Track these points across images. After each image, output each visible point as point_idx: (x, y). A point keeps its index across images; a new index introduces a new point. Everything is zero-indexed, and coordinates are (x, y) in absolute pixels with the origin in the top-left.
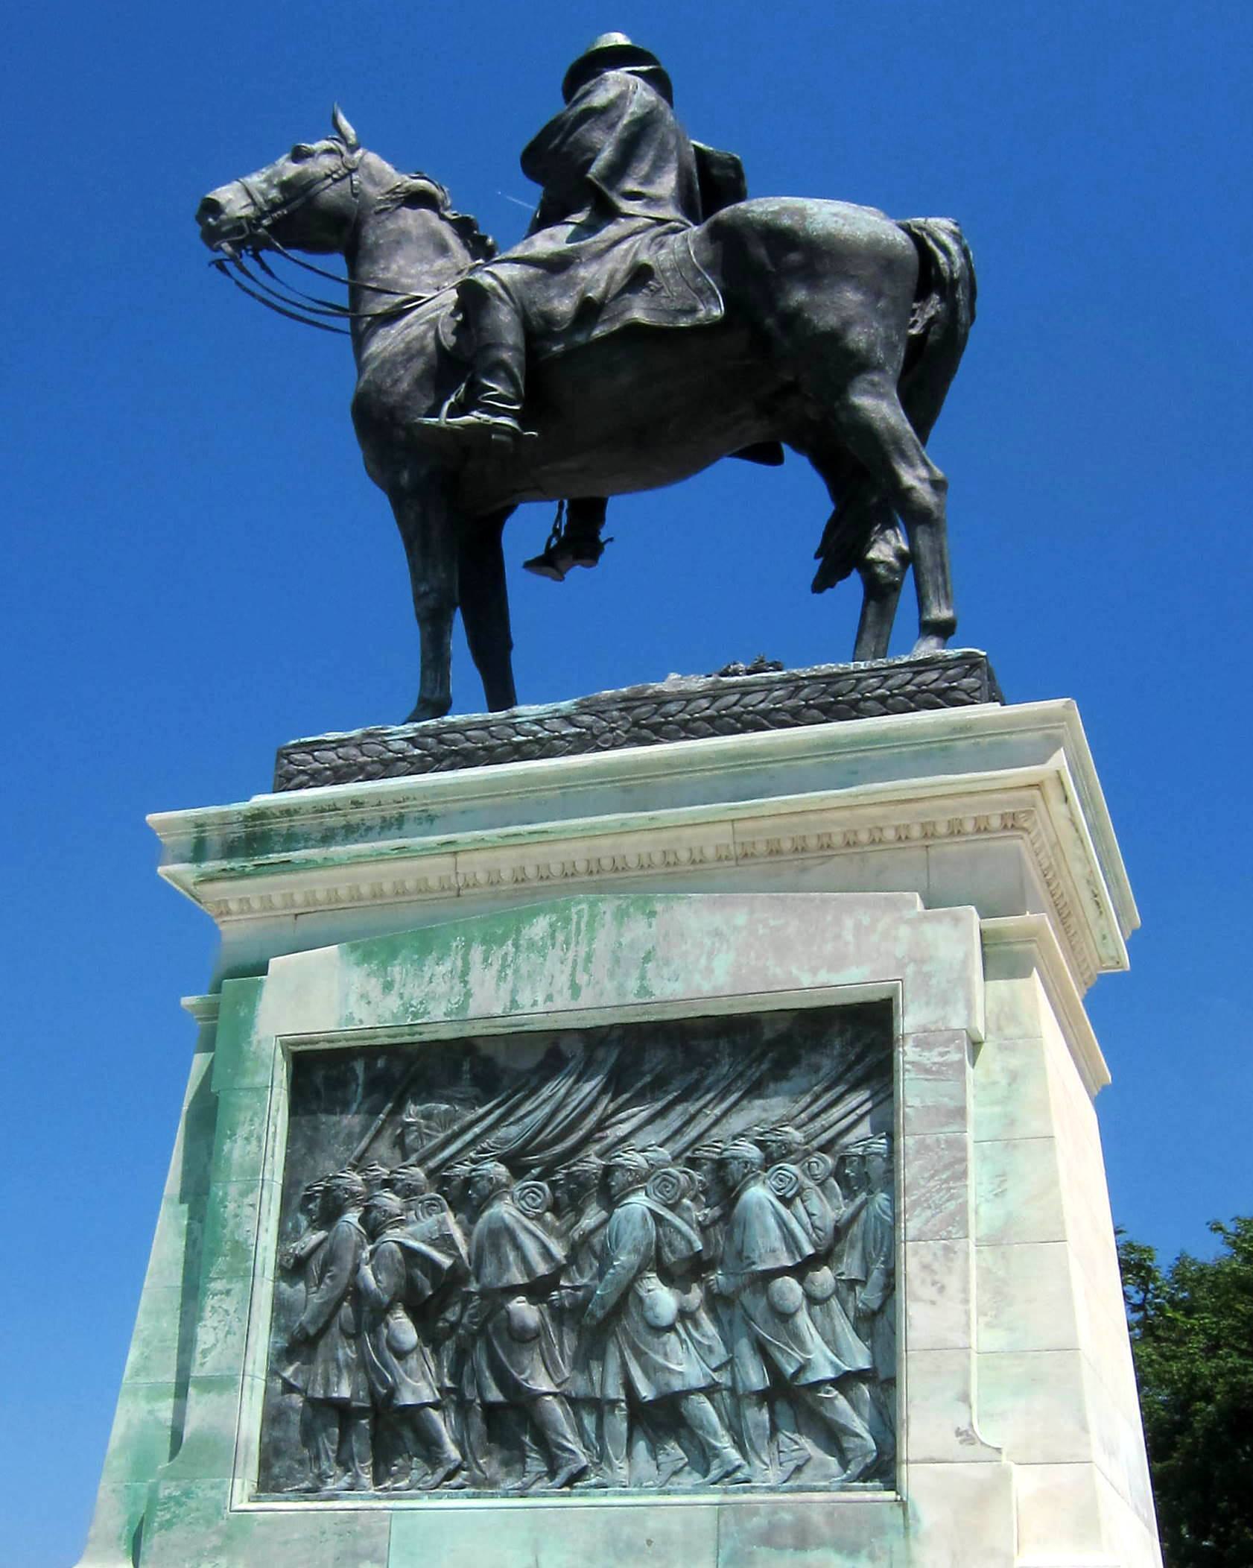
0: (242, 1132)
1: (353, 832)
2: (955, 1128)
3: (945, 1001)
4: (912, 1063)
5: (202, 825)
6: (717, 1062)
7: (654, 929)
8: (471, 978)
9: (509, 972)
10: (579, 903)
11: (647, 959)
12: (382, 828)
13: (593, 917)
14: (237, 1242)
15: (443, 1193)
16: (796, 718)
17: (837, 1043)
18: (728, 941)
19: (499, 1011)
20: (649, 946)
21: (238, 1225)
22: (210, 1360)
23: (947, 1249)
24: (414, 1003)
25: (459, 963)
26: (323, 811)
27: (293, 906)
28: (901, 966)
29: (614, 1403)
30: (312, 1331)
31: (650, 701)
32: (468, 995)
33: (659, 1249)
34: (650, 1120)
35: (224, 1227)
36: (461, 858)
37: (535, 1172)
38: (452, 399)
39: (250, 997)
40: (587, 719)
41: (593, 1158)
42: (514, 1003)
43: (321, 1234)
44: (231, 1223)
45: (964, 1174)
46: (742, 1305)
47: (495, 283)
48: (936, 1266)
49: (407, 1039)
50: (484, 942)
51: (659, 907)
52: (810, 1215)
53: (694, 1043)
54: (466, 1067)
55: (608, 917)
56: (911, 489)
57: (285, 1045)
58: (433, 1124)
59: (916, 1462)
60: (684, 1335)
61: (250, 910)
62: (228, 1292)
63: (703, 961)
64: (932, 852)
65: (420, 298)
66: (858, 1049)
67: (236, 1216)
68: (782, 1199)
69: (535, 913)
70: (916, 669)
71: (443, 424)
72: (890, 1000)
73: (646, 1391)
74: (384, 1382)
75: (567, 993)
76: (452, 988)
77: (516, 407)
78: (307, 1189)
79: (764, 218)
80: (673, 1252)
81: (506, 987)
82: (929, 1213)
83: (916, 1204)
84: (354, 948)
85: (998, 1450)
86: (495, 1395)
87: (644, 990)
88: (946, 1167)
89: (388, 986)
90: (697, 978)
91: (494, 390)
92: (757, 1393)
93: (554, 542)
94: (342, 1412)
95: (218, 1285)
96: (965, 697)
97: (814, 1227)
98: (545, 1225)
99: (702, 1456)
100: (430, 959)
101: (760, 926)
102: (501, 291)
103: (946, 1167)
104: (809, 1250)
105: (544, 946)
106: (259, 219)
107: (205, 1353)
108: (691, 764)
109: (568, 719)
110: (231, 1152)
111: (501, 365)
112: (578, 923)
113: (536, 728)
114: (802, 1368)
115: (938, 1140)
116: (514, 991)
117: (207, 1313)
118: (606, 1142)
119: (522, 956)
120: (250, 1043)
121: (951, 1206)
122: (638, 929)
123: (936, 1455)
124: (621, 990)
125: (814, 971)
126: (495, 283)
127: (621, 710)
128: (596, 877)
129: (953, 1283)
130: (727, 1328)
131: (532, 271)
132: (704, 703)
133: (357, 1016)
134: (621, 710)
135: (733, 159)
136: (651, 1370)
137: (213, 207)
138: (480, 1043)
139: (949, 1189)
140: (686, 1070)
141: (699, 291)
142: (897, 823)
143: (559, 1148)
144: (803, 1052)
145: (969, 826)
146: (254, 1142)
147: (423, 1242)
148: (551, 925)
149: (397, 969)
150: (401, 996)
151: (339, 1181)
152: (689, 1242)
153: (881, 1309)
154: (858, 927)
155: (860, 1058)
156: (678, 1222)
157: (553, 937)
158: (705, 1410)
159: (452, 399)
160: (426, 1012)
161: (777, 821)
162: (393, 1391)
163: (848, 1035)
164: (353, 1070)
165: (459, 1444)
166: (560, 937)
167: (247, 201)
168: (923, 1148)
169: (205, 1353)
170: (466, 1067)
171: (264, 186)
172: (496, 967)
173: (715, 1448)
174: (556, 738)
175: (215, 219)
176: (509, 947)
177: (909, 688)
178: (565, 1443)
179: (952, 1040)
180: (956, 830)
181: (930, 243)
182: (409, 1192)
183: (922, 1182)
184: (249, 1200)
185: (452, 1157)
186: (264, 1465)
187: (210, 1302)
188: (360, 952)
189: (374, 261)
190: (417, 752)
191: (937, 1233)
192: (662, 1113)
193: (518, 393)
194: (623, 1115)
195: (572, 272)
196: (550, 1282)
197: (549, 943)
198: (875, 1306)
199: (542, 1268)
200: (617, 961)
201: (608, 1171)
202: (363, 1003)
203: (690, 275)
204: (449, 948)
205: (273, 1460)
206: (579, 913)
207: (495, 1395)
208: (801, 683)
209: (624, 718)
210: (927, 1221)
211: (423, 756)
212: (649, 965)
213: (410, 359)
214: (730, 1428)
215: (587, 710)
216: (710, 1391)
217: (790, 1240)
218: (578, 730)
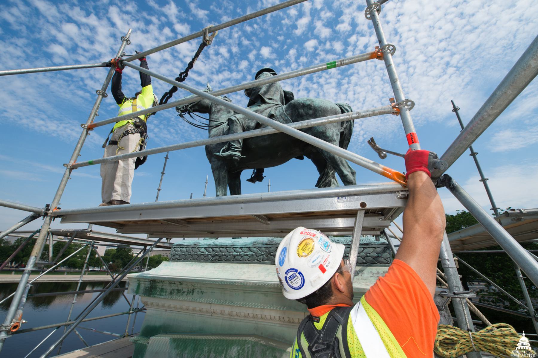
1: (179, 292)
12: (187, 293)
31: (274, 246)
38: (224, 148)
40: (255, 249)
47: (236, 119)
56: (347, 175)
71: (220, 155)
77: (240, 150)
79: (303, 102)
93: (253, 175)
102: (237, 121)
106: (188, 105)
113: (240, 250)
126: (236, 119)
127: (265, 247)
134: (265, 247)
135: (292, 93)
159: (224, 148)
181: (343, 108)
190: (207, 253)
193: (241, 146)
215: (254, 246)
218: (252, 253)
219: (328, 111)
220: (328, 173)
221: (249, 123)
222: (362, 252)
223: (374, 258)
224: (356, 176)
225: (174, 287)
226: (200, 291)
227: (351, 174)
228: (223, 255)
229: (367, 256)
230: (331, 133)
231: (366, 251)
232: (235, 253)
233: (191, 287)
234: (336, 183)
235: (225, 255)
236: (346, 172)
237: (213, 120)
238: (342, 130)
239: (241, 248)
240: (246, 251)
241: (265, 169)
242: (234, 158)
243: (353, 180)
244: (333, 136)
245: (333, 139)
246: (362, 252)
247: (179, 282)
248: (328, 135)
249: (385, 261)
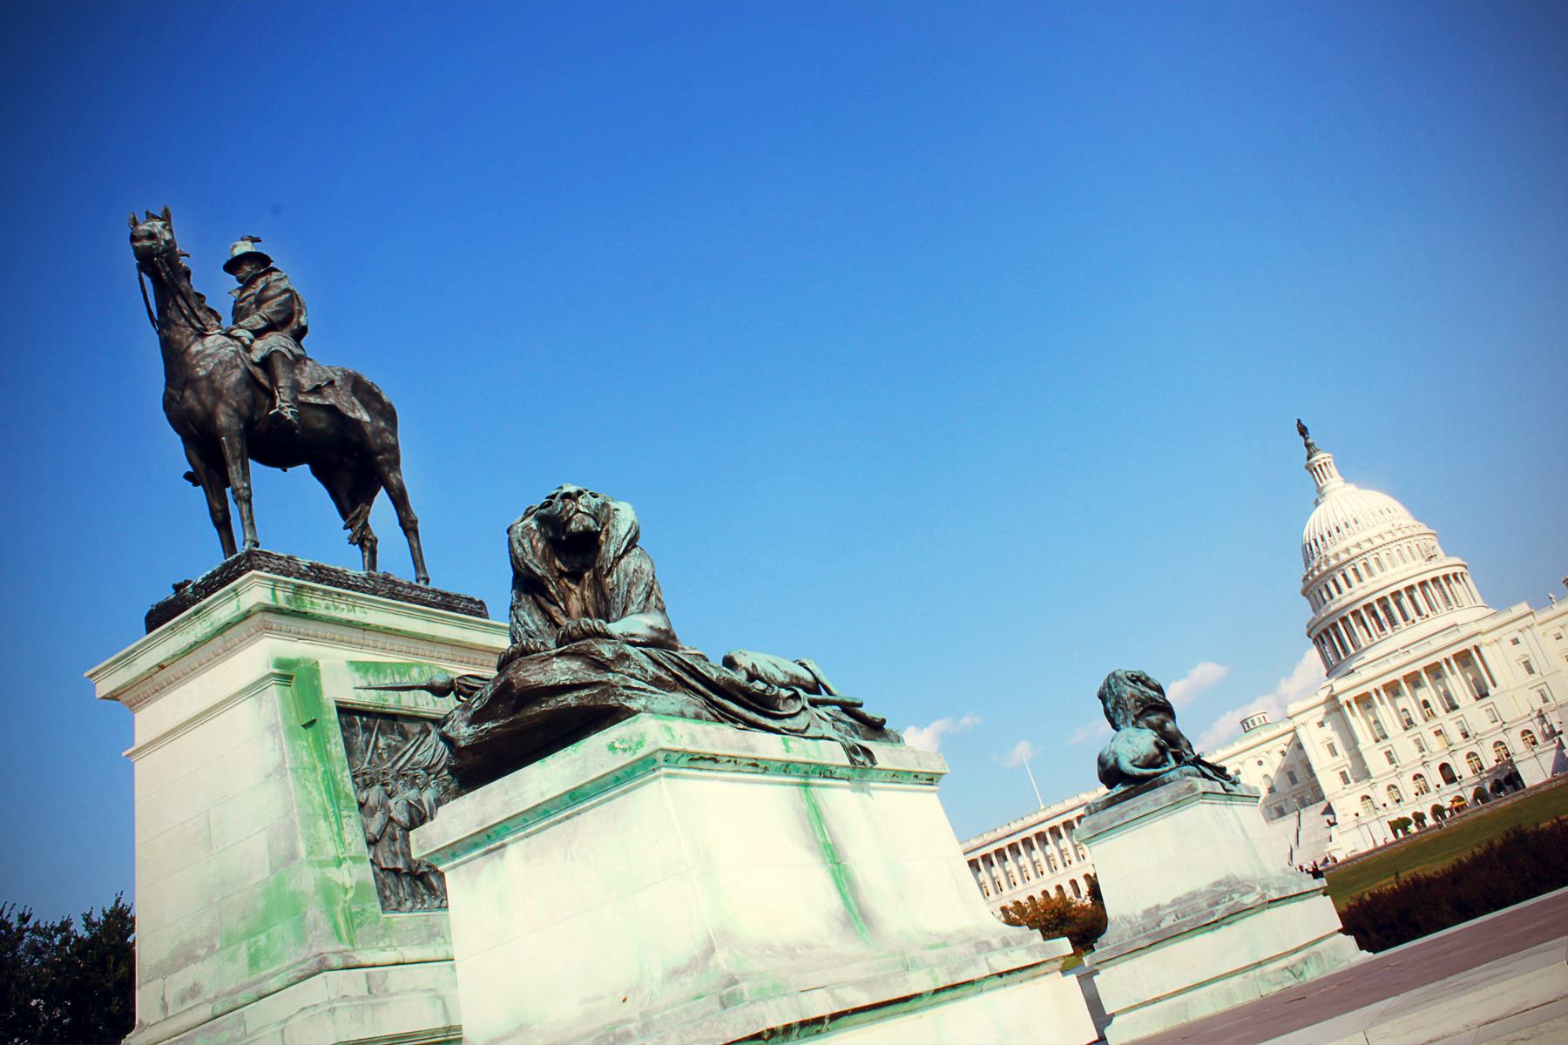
0: (333, 741)
42: (416, 703)
44: (341, 784)
107: (350, 844)
164: (355, 720)
169: (350, 844)
185: (402, 767)
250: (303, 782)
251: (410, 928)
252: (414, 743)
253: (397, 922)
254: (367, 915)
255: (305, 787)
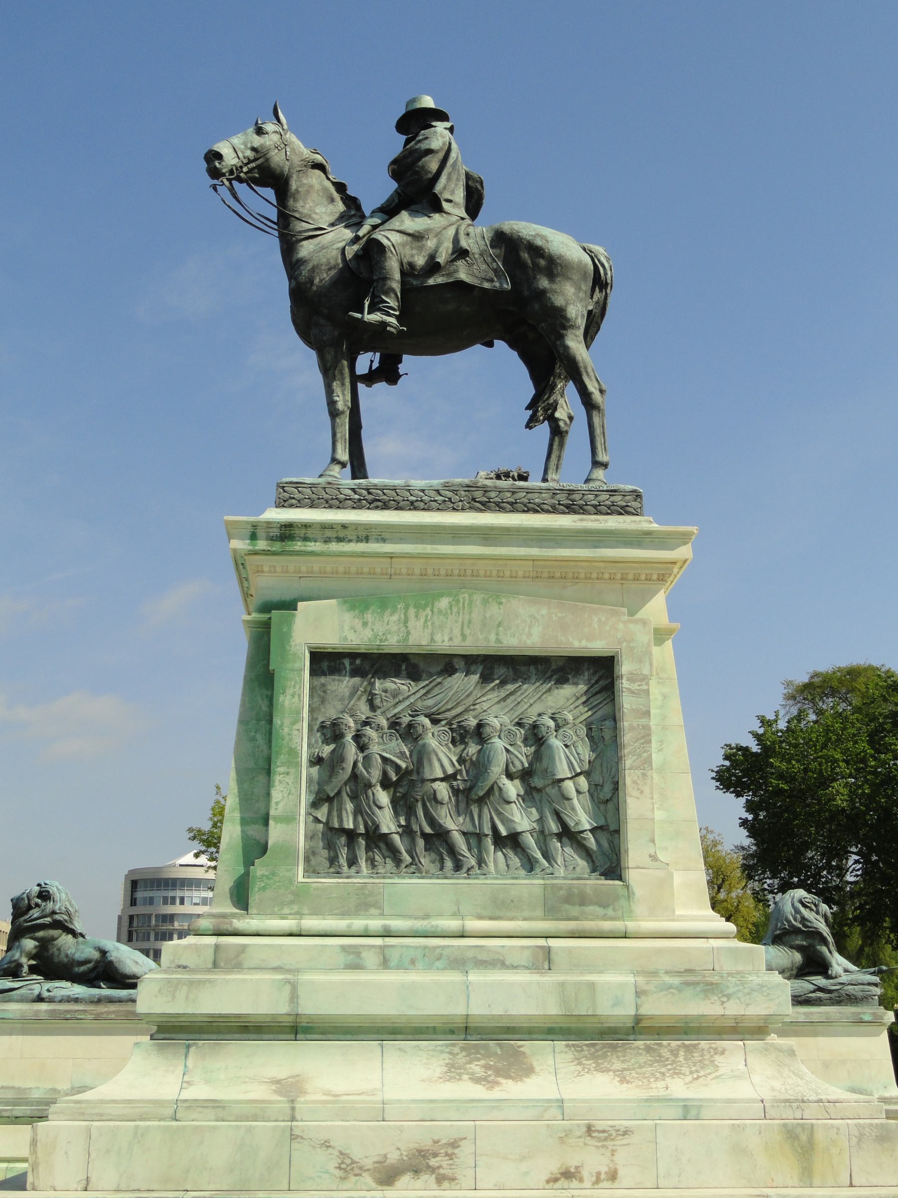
0: (289, 691)
2: (646, 720)
3: (640, 661)
4: (627, 688)
5: (255, 526)
6: (530, 677)
7: (502, 611)
8: (410, 624)
9: (429, 624)
10: (464, 593)
11: (499, 625)
13: (471, 602)
14: (291, 748)
15: (396, 730)
16: (554, 510)
17: (586, 674)
18: (538, 621)
19: (426, 644)
20: (500, 619)
21: (291, 740)
22: (280, 806)
23: (644, 775)
24: (380, 634)
25: (403, 616)
26: (325, 528)
27: (299, 572)
28: (620, 643)
29: (487, 835)
30: (332, 795)
32: (408, 633)
33: (507, 766)
34: (499, 702)
35: (283, 740)
36: (394, 560)
37: (443, 723)
39: (289, 623)
40: (447, 492)
41: (472, 719)
42: (432, 640)
43: (332, 746)
44: (287, 738)
45: (650, 742)
46: (546, 793)
47: (389, 244)
48: (639, 782)
49: (375, 651)
50: (415, 607)
51: (504, 600)
52: (578, 754)
53: (518, 667)
54: (404, 667)
55: (478, 603)
57: (309, 648)
58: (388, 695)
59: (632, 868)
60: (519, 806)
61: (275, 572)
62: (288, 773)
63: (527, 630)
64: (624, 586)
65: (325, 229)
66: (596, 678)
67: (289, 734)
68: (566, 746)
69: (441, 595)
70: (610, 493)
72: (613, 657)
73: (504, 833)
74: (374, 822)
75: (460, 638)
76: (400, 629)
77: (397, 313)
78: (323, 722)
80: (514, 767)
81: (429, 630)
82: (635, 757)
83: (629, 753)
84: (345, 602)
85: (668, 864)
86: (428, 830)
87: (498, 641)
88: (643, 737)
89: (365, 624)
90: (524, 637)
91: (387, 303)
92: (556, 834)
94: (351, 835)
95: (281, 769)
96: (634, 511)
97: (580, 759)
98: (449, 749)
99: (530, 865)
100: (387, 613)
101: (553, 616)
103: (643, 737)
104: (579, 770)
105: (447, 613)
106: (241, 167)
107: (277, 803)
108: (519, 532)
109: (438, 491)
110: (283, 701)
111: (393, 290)
112: (463, 603)
114: (577, 824)
115: (638, 725)
116: (432, 634)
117: (277, 783)
118: (476, 711)
119: (435, 617)
120: (291, 646)
121: (645, 755)
122: (495, 611)
123: (641, 866)
124: (487, 639)
125: (580, 640)
126: (389, 244)
127: (465, 491)
128: (463, 578)
129: (647, 790)
130: (538, 803)
131: (405, 238)
132: (509, 494)
133: (349, 638)
134: (465, 491)
135: (480, 178)
136: (506, 821)
137: (219, 156)
138: (411, 657)
139: (644, 747)
140: (515, 680)
141: (496, 271)
142: (610, 571)
143: (454, 713)
144: (570, 676)
145: (643, 577)
146: (297, 697)
147: (391, 754)
148: (450, 603)
149: (369, 616)
150: (373, 631)
151: (341, 720)
152: (522, 763)
153: (611, 799)
154: (600, 621)
155: (597, 682)
156: (516, 753)
157: (451, 609)
158: (530, 841)
160: (386, 640)
161: (555, 563)
162: (377, 827)
163: (591, 671)
164: (343, 664)
165: (410, 853)
166: (455, 610)
167: (234, 155)
168: (632, 728)
169: (277, 803)
170: (404, 667)
171: (243, 147)
172: (422, 620)
173: (536, 858)
174: (431, 501)
175: (220, 163)
176: (428, 611)
177: (608, 503)
178: (465, 854)
179: (643, 680)
180: (636, 579)
182: (379, 728)
183: (632, 743)
184: (296, 727)
186: (307, 860)
187: (277, 779)
188: (348, 605)
189: (295, 200)
190: (357, 497)
191: (639, 767)
192: (504, 699)
194: (484, 699)
195: (424, 242)
196: (453, 777)
197: (449, 611)
198: (608, 796)
199: (450, 771)
200: (484, 625)
201: (480, 726)
202: (352, 631)
203: (489, 260)
204: (397, 608)
205: (311, 857)
206: (463, 598)
207: (428, 830)
208: (555, 492)
209: (466, 496)
210: (634, 761)
211: (360, 500)
212: (501, 629)
213: (330, 269)
214: (540, 849)
216: (531, 832)
217: (570, 764)
219: (573, 268)
220: (554, 386)
221: (412, 256)
222: (607, 500)
223: (622, 507)
224: (606, 395)
225: (328, 533)
226: (379, 537)
227: (598, 391)
228: (390, 500)
229: (613, 505)
230: (574, 311)
231: (612, 499)
232: (414, 499)
233: (364, 534)
234: (565, 408)
235: (394, 500)
236: (592, 387)
237: (297, 215)
238: (590, 308)
239: (423, 491)
240: (432, 495)
241: (406, 358)
242: (388, 328)
243: (600, 403)
244: (576, 318)
245: (575, 325)
246: (607, 500)
247: (342, 526)
248: (569, 315)
249: (634, 511)
250: (253, 734)
251: (334, 895)
252: (427, 685)
253: (317, 889)
254: (277, 879)
255: (253, 739)
